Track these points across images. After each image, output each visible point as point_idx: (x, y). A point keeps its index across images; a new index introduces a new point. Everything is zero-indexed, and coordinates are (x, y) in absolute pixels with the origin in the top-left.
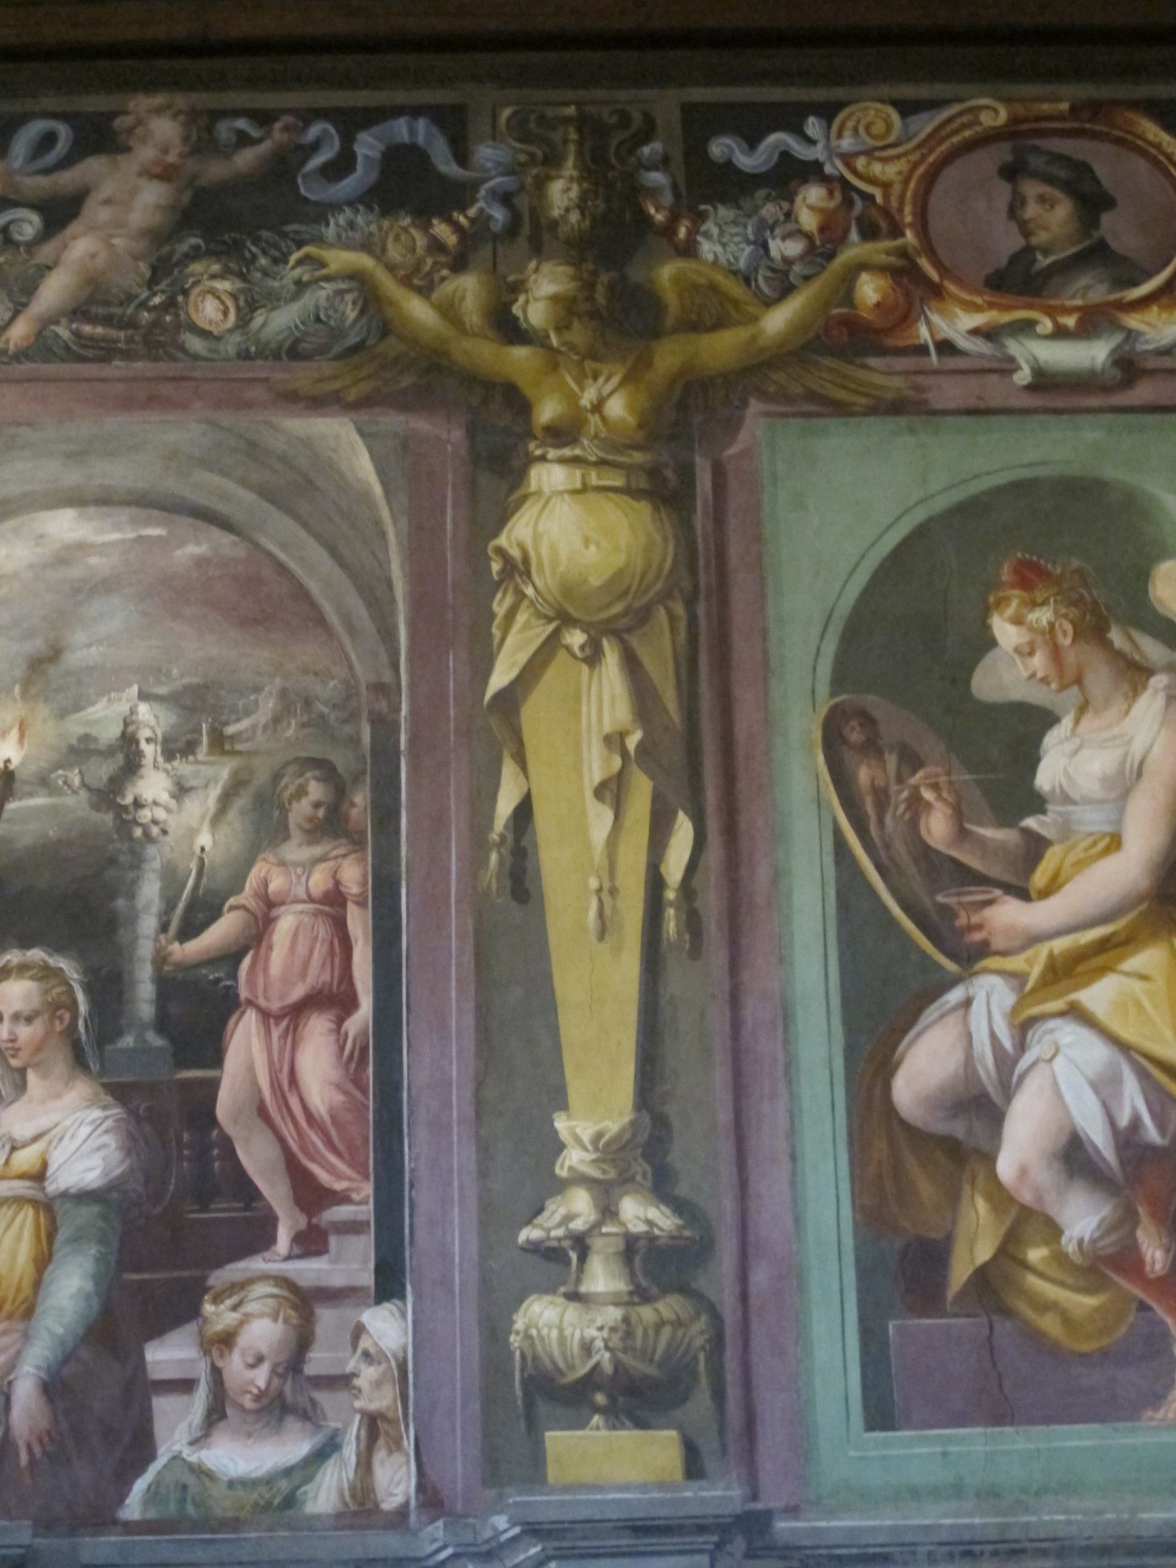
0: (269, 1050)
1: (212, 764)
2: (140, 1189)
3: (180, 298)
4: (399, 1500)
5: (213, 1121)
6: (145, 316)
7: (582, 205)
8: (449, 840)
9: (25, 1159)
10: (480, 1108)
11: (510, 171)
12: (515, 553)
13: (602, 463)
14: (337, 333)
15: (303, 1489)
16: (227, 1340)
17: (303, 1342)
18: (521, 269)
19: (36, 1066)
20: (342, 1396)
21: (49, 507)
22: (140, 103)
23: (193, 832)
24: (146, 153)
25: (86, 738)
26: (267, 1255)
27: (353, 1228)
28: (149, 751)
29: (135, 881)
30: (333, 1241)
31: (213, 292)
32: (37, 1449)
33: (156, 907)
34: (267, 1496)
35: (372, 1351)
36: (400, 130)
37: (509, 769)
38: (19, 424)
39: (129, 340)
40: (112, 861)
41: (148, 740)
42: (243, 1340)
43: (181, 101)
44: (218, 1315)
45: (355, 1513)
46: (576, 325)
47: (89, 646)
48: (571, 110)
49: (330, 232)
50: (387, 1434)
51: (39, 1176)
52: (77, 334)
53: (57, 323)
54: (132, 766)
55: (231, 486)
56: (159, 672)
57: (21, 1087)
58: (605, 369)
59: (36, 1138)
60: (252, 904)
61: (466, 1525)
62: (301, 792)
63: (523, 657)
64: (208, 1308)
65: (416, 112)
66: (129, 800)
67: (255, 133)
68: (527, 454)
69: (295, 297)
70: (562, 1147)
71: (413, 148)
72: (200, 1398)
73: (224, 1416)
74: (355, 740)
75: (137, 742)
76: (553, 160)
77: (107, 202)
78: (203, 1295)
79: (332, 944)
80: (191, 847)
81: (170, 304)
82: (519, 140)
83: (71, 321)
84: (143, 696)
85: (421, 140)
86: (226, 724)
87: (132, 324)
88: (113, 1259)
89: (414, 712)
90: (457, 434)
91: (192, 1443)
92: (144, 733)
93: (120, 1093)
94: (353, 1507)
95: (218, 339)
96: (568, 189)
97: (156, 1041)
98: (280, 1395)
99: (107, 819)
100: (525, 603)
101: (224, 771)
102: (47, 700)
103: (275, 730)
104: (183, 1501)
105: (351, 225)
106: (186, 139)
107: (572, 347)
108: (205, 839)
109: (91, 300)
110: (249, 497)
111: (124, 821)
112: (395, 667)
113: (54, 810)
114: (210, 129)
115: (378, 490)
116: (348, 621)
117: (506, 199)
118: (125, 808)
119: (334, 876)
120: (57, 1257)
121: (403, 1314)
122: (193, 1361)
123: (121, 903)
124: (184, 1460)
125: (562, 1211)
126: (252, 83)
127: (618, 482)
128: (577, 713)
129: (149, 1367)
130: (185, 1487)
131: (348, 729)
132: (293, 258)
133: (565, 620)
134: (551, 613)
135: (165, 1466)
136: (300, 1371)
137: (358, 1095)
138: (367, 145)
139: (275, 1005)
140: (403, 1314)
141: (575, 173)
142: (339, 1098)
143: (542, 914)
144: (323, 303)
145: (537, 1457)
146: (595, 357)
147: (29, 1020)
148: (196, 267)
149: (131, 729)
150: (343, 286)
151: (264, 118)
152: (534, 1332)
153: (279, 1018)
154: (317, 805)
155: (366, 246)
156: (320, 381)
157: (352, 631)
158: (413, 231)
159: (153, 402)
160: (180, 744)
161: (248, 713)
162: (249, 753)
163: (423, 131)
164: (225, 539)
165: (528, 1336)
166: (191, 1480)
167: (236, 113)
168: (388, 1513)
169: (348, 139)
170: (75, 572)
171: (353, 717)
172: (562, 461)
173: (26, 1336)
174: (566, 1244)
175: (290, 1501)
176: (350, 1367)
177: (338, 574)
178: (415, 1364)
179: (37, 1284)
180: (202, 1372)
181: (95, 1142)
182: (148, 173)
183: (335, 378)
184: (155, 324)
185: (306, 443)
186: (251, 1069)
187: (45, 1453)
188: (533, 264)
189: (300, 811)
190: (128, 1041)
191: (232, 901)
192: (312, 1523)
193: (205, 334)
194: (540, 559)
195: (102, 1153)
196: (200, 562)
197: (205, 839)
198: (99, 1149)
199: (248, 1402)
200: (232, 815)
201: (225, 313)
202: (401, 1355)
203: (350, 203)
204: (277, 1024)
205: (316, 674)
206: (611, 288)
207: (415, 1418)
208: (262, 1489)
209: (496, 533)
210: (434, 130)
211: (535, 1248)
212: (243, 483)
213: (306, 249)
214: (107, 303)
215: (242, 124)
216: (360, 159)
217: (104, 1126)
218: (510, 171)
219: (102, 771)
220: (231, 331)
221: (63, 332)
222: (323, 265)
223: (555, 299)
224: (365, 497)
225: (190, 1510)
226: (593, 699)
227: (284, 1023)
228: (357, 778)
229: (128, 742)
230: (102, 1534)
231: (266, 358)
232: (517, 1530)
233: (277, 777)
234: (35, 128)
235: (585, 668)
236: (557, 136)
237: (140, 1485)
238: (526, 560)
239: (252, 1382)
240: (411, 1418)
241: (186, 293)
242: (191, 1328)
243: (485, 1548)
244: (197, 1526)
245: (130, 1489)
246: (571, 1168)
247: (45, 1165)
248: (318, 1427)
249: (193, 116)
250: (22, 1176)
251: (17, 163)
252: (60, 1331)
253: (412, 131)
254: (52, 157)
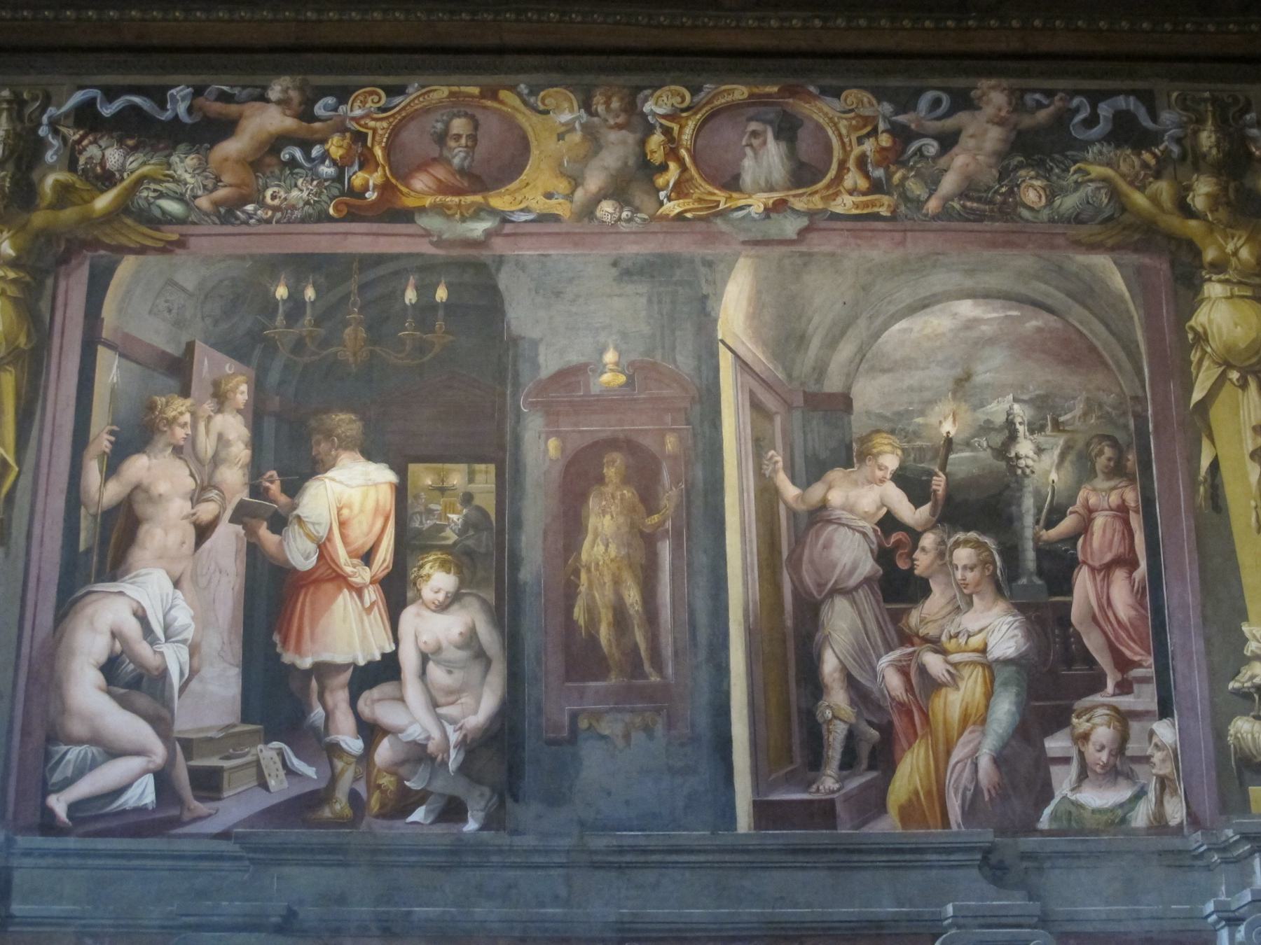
0: (1095, 585)
1: (1054, 436)
2: (1036, 659)
3: (1016, 189)
5: (1070, 625)
6: (999, 198)
7: (1218, 145)
8: (1178, 479)
9: (975, 641)
10: (1205, 619)
11: (1181, 126)
12: (1200, 329)
13: (1240, 283)
14: (1098, 210)
16: (1085, 737)
17: (1124, 738)
18: (1190, 179)
19: (977, 593)
20: (1146, 767)
21: (958, 299)
22: (984, 83)
23: (1048, 472)
24: (989, 111)
25: (988, 421)
26: (1103, 693)
27: (1144, 680)
28: (1021, 429)
29: (1020, 497)
30: (1135, 687)
31: (1032, 186)
32: (993, 792)
33: (1032, 511)
36: (1121, 102)
37: (1206, 443)
38: (939, 254)
39: (992, 211)
40: (1008, 486)
41: (1020, 423)
42: (1093, 737)
43: (1005, 83)
46: (1220, 209)
47: (986, 372)
48: (1207, 94)
49: (1090, 156)
51: (983, 650)
52: (964, 206)
53: (953, 200)
54: (1013, 437)
55: (1051, 290)
56: (1023, 387)
57: (970, 604)
58: (1238, 233)
59: (981, 631)
60: (1081, 510)
61: (1212, 834)
62: (1101, 453)
63: (1209, 384)
64: (1075, 720)
65: (1128, 93)
66: (1013, 455)
67: (1045, 102)
68: (1202, 277)
69: (1076, 190)
70: (1246, 640)
71: (1128, 112)
72: (1074, 769)
73: (1087, 776)
74: (1126, 427)
75: (1015, 424)
76: (1200, 121)
77: (972, 136)
79: (1123, 534)
80: (1047, 479)
81: (1011, 192)
82: (1182, 109)
83: (960, 200)
84: (1016, 400)
85: (1132, 107)
86: (1060, 416)
87: (991, 202)
89: (1155, 414)
90: (1165, 266)
91: (1073, 790)
92: (1018, 420)
93: (1021, 608)
94: (1155, 824)
95: (1038, 211)
96: (1210, 137)
97: (1038, 581)
98: (1115, 766)
99: (1002, 465)
100: (1207, 356)
101: (1061, 441)
102: (965, 401)
103: (1085, 421)
104: (1069, 820)
105: (1101, 153)
106: (1010, 103)
107: (1220, 221)
108: (1054, 476)
109: (969, 188)
110: (1061, 296)
111: (1012, 466)
112: (1144, 387)
113: (975, 459)
114: (1022, 98)
115: (1127, 295)
116: (1117, 363)
117: (1179, 141)
118: (1011, 458)
119: (1122, 497)
120: (996, 693)
123: (1014, 508)
125: (1249, 673)
126: (1043, 74)
127: (1249, 293)
128: (1237, 414)
130: (1070, 813)
131: (1122, 421)
132: (1072, 169)
133: (1229, 366)
134: (1221, 362)
136: (1124, 754)
137: (1143, 612)
138: (1105, 110)
139: (1097, 564)
141: (1213, 128)
142: (1133, 613)
143: (1228, 516)
144: (1090, 193)
145: (1246, 801)
146: (1231, 227)
147: (972, 569)
148: (1023, 173)
149: (1011, 417)
150: (1099, 185)
151: (1050, 94)
152: (1239, 735)
153: (1100, 571)
154: (1109, 459)
155: (1109, 164)
156: (1091, 235)
157: (1120, 368)
158: (1133, 157)
159: (1008, 244)
160: (1037, 426)
161: (1070, 410)
162: (1072, 431)
163: (1132, 103)
164: (1052, 318)
165: (1236, 738)
166: (1073, 809)
167: (1034, 91)
169: (1094, 107)
170: (974, 334)
171: (1124, 414)
172: (1220, 281)
173: (984, 734)
174: (1252, 690)
175: (1124, 820)
176: (1149, 752)
177: (1112, 339)
179: (987, 707)
180: (1074, 753)
181: (1011, 633)
182: (990, 121)
183: (1100, 234)
184: (1004, 202)
185: (1088, 268)
186: (1087, 597)
187: (997, 794)
188: (1195, 176)
189: (1101, 462)
190: (1024, 581)
191: (1071, 509)
192: (1135, 832)
193: (1031, 209)
194: (1212, 332)
195: (1015, 639)
196: (1039, 330)
197: (1054, 476)
198: (1013, 637)
199: (1098, 769)
200: (1067, 464)
201: (1040, 197)
203: (1099, 141)
204: (1099, 573)
205: (1104, 391)
206: (1237, 190)
208: (1110, 814)
209: (1190, 318)
210: (1139, 104)
211: (1236, 692)
212: (1057, 288)
213: (1078, 165)
214: (979, 191)
215: (1038, 96)
216: (1101, 117)
217: (1015, 625)
218: (1181, 126)
219: (998, 439)
220: (1045, 207)
221: (956, 205)
222: (1089, 174)
223: (1208, 195)
224: (1121, 298)
226: (1246, 408)
227: (1102, 574)
228: (1129, 446)
229: (1010, 424)
231: (1063, 222)
232: (1237, 837)
233: (1088, 444)
234: (929, 96)
235: (1240, 391)
236: (1202, 107)
237: (1047, 811)
238: (1205, 333)
239: (1100, 759)
241: (1018, 186)
242: (1067, 730)
243: (1222, 846)
244: (1081, 832)
246: (1252, 651)
247: (986, 645)
248: (1135, 783)
249: (1011, 92)
250: (974, 651)
251: (922, 114)
252: (1001, 731)
253: (1128, 104)
254: (940, 111)
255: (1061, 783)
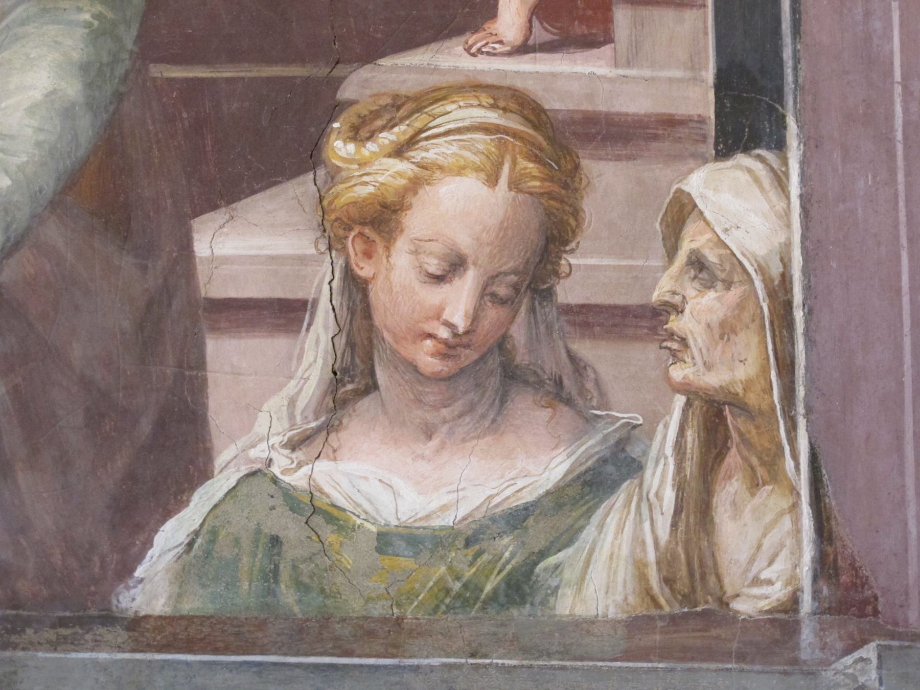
4: (777, 592)
15: (552, 560)
34: (468, 573)
35: (712, 257)
44: (362, 164)
45: (673, 619)
50: (745, 441)
73: (372, 387)
78: (331, 120)
88: (129, 38)
91: (293, 445)
98: (502, 344)
121: (781, 181)
122: (302, 260)
124: (275, 480)
129: (202, 271)
130: (275, 541)
135: (231, 492)
136: (548, 294)
140: (781, 181)
168: (750, 624)
176: (660, 292)
178: (808, 289)
202: (776, 269)
207: (809, 410)
208: (458, 557)
225: (288, 596)
230: (74, 643)
239: (437, 315)
240: (801, 409)
245: (148, 544)
255: (251, 410)
